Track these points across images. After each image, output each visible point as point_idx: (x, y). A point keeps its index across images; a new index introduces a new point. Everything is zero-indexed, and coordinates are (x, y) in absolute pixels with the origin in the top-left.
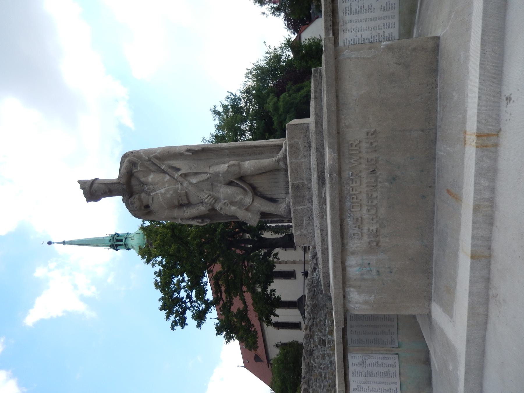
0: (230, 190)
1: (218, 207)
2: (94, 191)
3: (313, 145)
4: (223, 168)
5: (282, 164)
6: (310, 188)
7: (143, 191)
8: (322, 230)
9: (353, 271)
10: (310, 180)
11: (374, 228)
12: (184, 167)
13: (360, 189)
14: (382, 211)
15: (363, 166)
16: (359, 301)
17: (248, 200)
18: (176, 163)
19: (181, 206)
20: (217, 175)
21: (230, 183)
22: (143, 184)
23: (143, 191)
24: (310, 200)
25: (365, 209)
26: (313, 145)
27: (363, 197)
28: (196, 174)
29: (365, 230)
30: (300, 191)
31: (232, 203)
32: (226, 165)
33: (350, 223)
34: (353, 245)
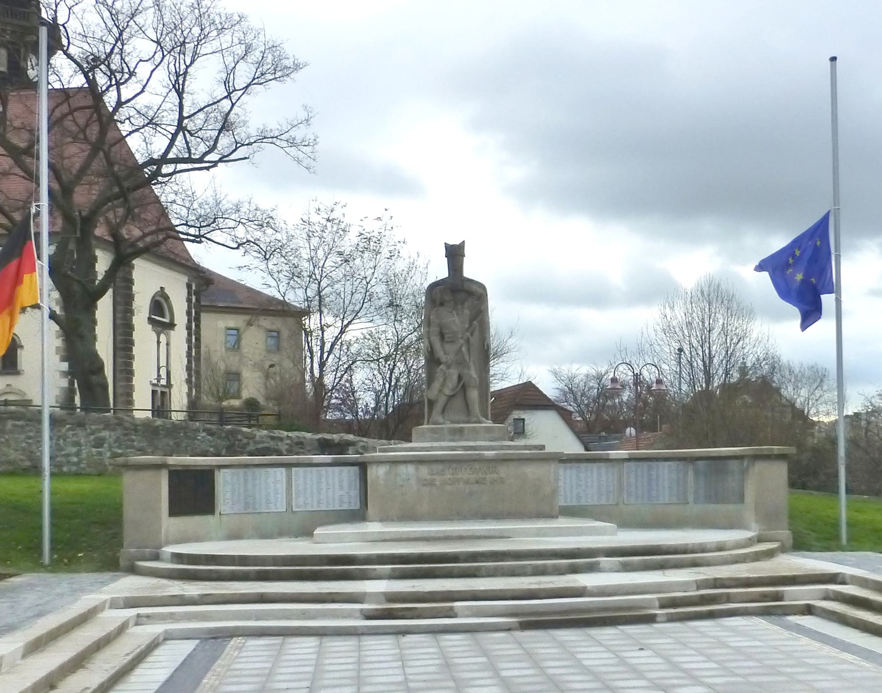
0: (455, 378)
1: (442, 367)
2: (455, 254)
3: (493, 444)
4: (474, 373)
5: (474, 419)
6: (460, 440)
7: (456, 304)
8: (431, 447)
9: (402, 469)
10: (467, 440)
11: (438, 483)
12: (475, 340)
13: (465, 474)
14: (448, 488)
15: (481, 476)
16: (376, 473)
17: (447, 392)
18: (477, 333)
19: (442, 336)
20: (468, 368)
21: (460, 378)
22: (463, 304)
23: (456, 304)
24: (451, 441)
25: (449, 476)
26: (493, 444)
27: (460, 476)
28: (469, 350)
29: (434, 477)
30: (459, 433)
31: (445, 380)
32: (475, 376)
33: (439, 467)
34: (424, 471)
